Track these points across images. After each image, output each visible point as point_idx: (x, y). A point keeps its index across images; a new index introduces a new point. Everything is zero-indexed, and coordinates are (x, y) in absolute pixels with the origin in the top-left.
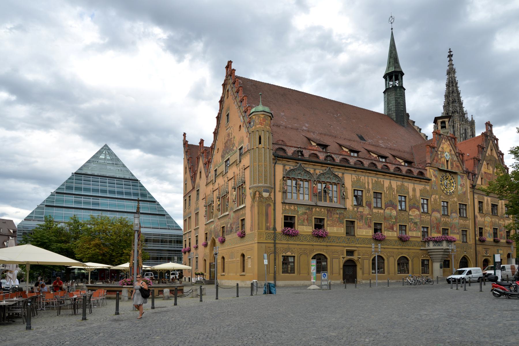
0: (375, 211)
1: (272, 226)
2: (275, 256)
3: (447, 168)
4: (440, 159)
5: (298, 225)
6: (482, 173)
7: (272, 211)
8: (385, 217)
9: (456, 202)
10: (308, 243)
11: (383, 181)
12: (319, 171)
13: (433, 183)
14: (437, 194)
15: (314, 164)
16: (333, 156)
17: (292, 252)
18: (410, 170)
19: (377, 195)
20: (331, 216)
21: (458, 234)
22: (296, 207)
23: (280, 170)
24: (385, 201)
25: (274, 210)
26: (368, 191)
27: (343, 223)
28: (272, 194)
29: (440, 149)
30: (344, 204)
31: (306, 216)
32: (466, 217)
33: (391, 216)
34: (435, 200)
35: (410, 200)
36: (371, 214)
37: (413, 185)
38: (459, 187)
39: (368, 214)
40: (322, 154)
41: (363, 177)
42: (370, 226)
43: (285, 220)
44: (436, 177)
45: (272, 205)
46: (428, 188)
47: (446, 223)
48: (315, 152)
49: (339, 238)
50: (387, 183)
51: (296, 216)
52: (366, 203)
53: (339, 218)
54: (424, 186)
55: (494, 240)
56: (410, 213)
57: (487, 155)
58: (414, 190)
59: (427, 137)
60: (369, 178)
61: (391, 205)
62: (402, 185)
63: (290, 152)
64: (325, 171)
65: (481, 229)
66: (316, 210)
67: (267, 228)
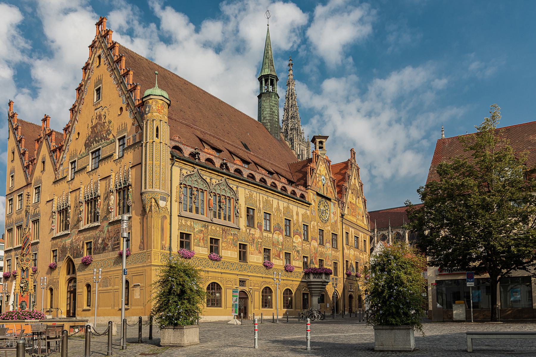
0: (265, 234)
1: (167, 245)
4: (318, 183)
7: (169, 226)
12: (215, 180)
15: (211, 171)
16: (228, 165)
18: (294, 191)
25: (171, 224)
28: (169, 203)
29: (318, 172)
30: (238, 224)
33: (278, 242)
35: (294, 224)
39: (259, 238)
42: (260, 252)
44: (314, 201)
46: (308, 212)
47: (322, 254)
48: (212, 157)
49: (232, 264)
50: (275, 202)
51: (192, 233)
53: (233, 240)
54: (305, 210)
58: (297, 214)
61: (278, 229)
62: (288, 207)
64: (221, 182)
67: (163, 248)
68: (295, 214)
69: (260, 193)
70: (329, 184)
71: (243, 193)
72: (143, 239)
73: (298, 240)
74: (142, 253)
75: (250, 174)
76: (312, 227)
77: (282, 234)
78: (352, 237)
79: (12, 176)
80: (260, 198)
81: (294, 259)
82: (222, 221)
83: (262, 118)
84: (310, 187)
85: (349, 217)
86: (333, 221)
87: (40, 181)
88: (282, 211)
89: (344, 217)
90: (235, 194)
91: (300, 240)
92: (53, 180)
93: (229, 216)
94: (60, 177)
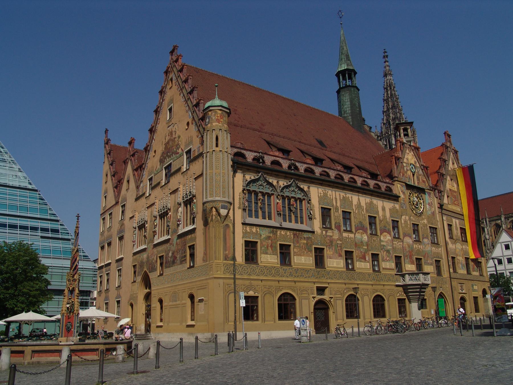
0: (345, 235)
1: (230, 256)
2: (235, 297)
5: (261, 253)
6: (447, 190)
7: (232, 234)
8: (356, 243)
9: (426, 225)
10: (273, 279)
11: (352, 197)
13: (402, 201)
14: (406, 215)
15: (277, 173)
17: (255, 291)
19: (346, 215)
21: (431, 264)
22: (258, 230)
24: (355, 222)
25: (234, 233)
26: (337, 209)
27: (311, 251)
30: (312, 226)
32: (437, 244)
33: (362, 242)
34: (405, 221)
35: (381, 221)
36: (341, 239)
37: (382, 202)
39: (338, 239)
40: (285, 161)
42: (340, 255)
43: (245, 246)
44: (404, 193)
45: (231, 226)
48: (277, 159)
49: (307, 271)
52: (335, 225)
53: (307, 244)
54: (393, 205)
55: (480, 275)
56: (382, 238)
57: (450, 169)
58: (384, 209)
60: (337, 193)
61: (361, 227)
62: (371, 203)
63: (250, 156)
65: (453, 258)
66: (280, 233)
67: (226, 258)
68: (380, 209)
69: (335, 191)
71: (315, 192)
72: (206, 249)
73: (386, 238)
74: (205, 265)
75: (323, 171)
76: (403, 222)
77: (366, 233)
78: (457, 229)
79: (105, 197)
80: (336, 196)
81: (383, 260)
82: (293, 225)
84: (396, 179)
85: (451, 207)
86: (430, 213)
87: (125, 199)
88: (365, 207)
89: (444, 207)
90: (306, 194)
91: (389, 237)
92: (135, 197)
93: (302, 217)
94: (141, 194)
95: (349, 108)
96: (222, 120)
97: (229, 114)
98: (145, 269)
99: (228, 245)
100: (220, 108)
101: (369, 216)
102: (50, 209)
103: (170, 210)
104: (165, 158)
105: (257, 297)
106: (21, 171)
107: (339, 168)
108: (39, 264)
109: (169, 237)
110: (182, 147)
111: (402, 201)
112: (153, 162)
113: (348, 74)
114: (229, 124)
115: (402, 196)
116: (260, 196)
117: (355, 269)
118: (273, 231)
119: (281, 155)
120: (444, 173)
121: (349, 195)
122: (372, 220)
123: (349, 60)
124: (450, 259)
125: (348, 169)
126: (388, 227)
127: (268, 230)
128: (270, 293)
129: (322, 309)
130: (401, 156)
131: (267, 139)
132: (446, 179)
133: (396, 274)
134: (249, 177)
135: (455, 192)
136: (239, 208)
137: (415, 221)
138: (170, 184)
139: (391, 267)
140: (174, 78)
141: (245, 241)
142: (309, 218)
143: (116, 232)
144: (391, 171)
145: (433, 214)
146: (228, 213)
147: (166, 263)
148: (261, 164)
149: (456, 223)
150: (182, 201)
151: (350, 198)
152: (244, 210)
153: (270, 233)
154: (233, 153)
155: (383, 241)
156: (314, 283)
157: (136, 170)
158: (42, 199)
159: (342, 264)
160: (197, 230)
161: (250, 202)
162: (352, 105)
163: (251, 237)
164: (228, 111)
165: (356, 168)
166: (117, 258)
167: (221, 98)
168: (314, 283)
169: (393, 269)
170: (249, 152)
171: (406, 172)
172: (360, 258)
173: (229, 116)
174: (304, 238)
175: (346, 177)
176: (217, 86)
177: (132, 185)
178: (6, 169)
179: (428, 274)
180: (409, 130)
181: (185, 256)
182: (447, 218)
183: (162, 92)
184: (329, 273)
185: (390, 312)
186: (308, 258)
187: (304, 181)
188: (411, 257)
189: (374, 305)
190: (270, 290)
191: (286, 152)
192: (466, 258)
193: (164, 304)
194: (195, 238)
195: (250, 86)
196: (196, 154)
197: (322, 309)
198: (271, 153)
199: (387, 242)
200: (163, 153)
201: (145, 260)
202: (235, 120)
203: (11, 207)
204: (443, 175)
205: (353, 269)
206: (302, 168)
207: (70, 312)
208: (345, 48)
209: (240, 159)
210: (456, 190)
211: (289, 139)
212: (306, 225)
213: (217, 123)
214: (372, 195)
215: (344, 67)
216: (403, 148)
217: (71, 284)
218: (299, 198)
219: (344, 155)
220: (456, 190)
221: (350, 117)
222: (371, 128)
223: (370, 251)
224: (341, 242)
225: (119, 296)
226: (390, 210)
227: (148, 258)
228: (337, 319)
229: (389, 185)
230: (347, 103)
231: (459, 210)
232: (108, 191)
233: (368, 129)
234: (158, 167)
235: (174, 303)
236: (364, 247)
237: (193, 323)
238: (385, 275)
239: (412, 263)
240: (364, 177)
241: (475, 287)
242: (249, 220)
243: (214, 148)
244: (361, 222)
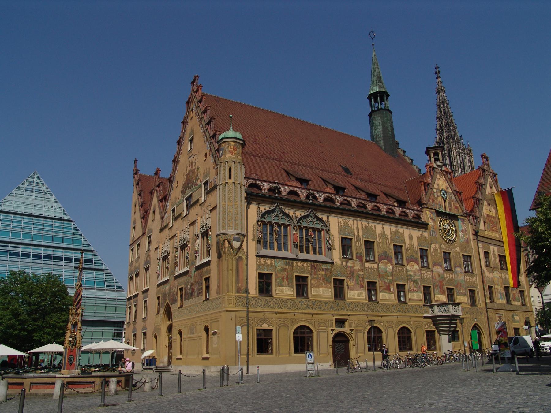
0: (367, 265)
1: (243, 288)
2: (248, 330)
3: (446, 210)
5: (275, 286)
7: (245, 267)
8: (379, 274)
9: (459, 253)
10: (289, 311)
11: (375, 226)
13: (432, 229)
14: (436, 243)
17: (269, 323)
19: (369, 245)
20: (315, 274)
21: (465, 294)
22: (273, 262)
23: (254, 212)
25: (247, 265)
26: (358, 238)
27: (330, 282)
30: (331, 256)
31: (285, 273)
32: (472, 273)
33: (386, 272)
34: (435, 250)
35: (407, 250)
36: (363, 269)
38: (461, 233)
40: (303, 191)
41: (351, 222)
42: (362, 287)
43: (259, 278)
44: (433, 220)
48: (295, 189)
49: (326, 303)
52: (357, 255)
53: (326, 275)
54: (421, 233)
56: (409, 268)
58: (411, 238)
59: (420, 170)
60: (359, 222)
61: (385, 257)
62: (397, 231)
63: (265, 187)
66: (297, 265)
67: (239, 290)
69: (357, 220)
70: (453, 198)
71: (335, 223)
72: (219, 282)
73: (413, 268)
76: (432, 250)
78: (495, 257)
79: (134, 228)
80: (357, 226)
81: (410, 291)
82: (311, 256)
83: (375, 136)
84: (425, 206)
85: (488, 234)
87: (151, 231)
88: (389, 236)
89: (479, 234)
91: (416, 267)
93: (320, 248)
94: (165, 225)
95: (382, 132)
96: (235, 152)
97: (243, 146)
98: (167, 301)
99: (241, 277)
100: (233, 140)
101: (394, 245)
102: (85, 240)
103: (189, 241)
104: (186, 189)
105: (272, 330)
106: (56, 202)
107: (361, 196)
108: (67, 295)
109: (188, 269)
110: (201, 178)
111: (432, 229)
112: (176, 193)
113: (381, 96)
114: (244, 154)
115: (431, 223)
116: (276, 228)
117: (379, 300)
118: (289, 263)
119: (299, 185)
120: (481, 198)
121: (372, 224)
122: (398, 249)
123: (381, 82)
124: (486, 288)
125: (372, 197)
126: (415, 256)
127: (283, 262)
128: (285, 326)
129: (341, 343)
130: (430, 182)
131: (286, 169)
132: (482, 204)
133: (424, 305)
134: (264, 208)
135: (493, 217)
136: (253, 240)
137: (445, 250)
138: (190, 216)
139: (418, 298)
140: (195, 109)
141: (259, 273)
142: (328, 249)
143: (143, 263)
144: (421, 199)
145: (467, 241)
146: (241, 245)
147: (185, 295)
148: (277, 195)
149: (494, 250)
150: (199, 233)
151: (373, 227)
152: (259, 242)
153: (286, 264)
154: (247, 184)
155: (410, 271)
156: (333, 315)
157: (161, 201)
158: (77, 230)
159: (364, 295)
160: (212, 262)
161: (265, 233)
162: (385, 129)
163: (266, 269)
164: (242, 142)
165: (383, 195)
166: (144, 289)
167: (235, 130)
168: (333, 315)
169: (421, 300)
170: (264, 183)
171: (437, 199)
172: (384, 289)
173: (243, 147)
174: (323, 269)
175: (370, 206)
176: (231, 117)
177: (158, 216)
178: (41, 200)
179: (459, 304)
180: (440, 155)
181: (202, 289)
182: (482, 245)
183: (184, 123)
184: (349, 304)
185: (417, 344)
186: (326, 289)
187: (323, 211)
188: (441, 287)
189: (399, 338)
190: (285, 322)
191: (304, 182)
192: (505, 287)
193: (183, 336)
194: (210, 270)
195: (274, 113)
196: (213, 186)
197: (341, 343)
198: (288, 183)
199: (414, 272)
200: (185, 184)
201: (167, 292)
202: (255, 150)
203: (46, 238)
204: (479, 200)
205: (376, 300)
206: (321, 197)
207: (73, 345)
208: (377, 69)
209: (255, 191)
210: (494, 215)
211: (311, 167)
212: (325, 256)
213: (230, 155)
214: (397, 223)
215: (376, 89)
216: (434, 173)
217: (74, 318)
218: (317, 229)
219: (371, 182)
220: (494, 215)
221: (382, 142)
222: (404, 152)
223: (395, 281)
224: (363, 273)
225: (145, 328)
226: (418, 238)
227: (170, 289)
228: (357, 352)
229: (417, 212)
230: (379, 127)
231: (498, 236)
232: (137, 221)
233: (402, 153)
234: (180, 198)
235: (192, 336)
236: (389, 278)
237: (207, 356)
238: (412, 306)
239: (443, 293)
240: (390, 205)
241: (516, 318)
242: (264, 252)
243: (227, 180)
244: (385, 252)
